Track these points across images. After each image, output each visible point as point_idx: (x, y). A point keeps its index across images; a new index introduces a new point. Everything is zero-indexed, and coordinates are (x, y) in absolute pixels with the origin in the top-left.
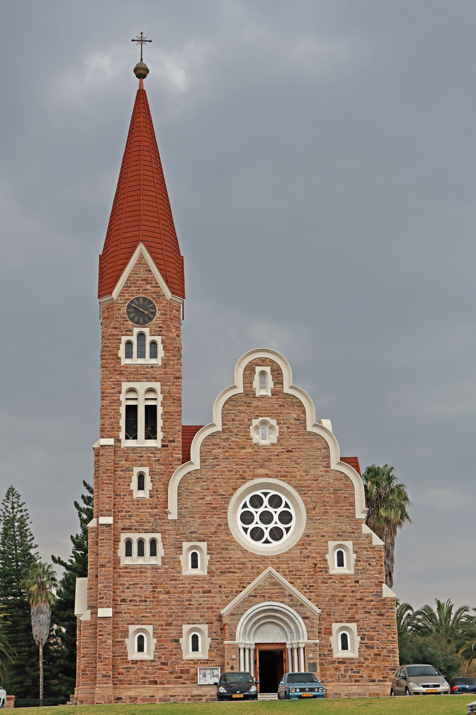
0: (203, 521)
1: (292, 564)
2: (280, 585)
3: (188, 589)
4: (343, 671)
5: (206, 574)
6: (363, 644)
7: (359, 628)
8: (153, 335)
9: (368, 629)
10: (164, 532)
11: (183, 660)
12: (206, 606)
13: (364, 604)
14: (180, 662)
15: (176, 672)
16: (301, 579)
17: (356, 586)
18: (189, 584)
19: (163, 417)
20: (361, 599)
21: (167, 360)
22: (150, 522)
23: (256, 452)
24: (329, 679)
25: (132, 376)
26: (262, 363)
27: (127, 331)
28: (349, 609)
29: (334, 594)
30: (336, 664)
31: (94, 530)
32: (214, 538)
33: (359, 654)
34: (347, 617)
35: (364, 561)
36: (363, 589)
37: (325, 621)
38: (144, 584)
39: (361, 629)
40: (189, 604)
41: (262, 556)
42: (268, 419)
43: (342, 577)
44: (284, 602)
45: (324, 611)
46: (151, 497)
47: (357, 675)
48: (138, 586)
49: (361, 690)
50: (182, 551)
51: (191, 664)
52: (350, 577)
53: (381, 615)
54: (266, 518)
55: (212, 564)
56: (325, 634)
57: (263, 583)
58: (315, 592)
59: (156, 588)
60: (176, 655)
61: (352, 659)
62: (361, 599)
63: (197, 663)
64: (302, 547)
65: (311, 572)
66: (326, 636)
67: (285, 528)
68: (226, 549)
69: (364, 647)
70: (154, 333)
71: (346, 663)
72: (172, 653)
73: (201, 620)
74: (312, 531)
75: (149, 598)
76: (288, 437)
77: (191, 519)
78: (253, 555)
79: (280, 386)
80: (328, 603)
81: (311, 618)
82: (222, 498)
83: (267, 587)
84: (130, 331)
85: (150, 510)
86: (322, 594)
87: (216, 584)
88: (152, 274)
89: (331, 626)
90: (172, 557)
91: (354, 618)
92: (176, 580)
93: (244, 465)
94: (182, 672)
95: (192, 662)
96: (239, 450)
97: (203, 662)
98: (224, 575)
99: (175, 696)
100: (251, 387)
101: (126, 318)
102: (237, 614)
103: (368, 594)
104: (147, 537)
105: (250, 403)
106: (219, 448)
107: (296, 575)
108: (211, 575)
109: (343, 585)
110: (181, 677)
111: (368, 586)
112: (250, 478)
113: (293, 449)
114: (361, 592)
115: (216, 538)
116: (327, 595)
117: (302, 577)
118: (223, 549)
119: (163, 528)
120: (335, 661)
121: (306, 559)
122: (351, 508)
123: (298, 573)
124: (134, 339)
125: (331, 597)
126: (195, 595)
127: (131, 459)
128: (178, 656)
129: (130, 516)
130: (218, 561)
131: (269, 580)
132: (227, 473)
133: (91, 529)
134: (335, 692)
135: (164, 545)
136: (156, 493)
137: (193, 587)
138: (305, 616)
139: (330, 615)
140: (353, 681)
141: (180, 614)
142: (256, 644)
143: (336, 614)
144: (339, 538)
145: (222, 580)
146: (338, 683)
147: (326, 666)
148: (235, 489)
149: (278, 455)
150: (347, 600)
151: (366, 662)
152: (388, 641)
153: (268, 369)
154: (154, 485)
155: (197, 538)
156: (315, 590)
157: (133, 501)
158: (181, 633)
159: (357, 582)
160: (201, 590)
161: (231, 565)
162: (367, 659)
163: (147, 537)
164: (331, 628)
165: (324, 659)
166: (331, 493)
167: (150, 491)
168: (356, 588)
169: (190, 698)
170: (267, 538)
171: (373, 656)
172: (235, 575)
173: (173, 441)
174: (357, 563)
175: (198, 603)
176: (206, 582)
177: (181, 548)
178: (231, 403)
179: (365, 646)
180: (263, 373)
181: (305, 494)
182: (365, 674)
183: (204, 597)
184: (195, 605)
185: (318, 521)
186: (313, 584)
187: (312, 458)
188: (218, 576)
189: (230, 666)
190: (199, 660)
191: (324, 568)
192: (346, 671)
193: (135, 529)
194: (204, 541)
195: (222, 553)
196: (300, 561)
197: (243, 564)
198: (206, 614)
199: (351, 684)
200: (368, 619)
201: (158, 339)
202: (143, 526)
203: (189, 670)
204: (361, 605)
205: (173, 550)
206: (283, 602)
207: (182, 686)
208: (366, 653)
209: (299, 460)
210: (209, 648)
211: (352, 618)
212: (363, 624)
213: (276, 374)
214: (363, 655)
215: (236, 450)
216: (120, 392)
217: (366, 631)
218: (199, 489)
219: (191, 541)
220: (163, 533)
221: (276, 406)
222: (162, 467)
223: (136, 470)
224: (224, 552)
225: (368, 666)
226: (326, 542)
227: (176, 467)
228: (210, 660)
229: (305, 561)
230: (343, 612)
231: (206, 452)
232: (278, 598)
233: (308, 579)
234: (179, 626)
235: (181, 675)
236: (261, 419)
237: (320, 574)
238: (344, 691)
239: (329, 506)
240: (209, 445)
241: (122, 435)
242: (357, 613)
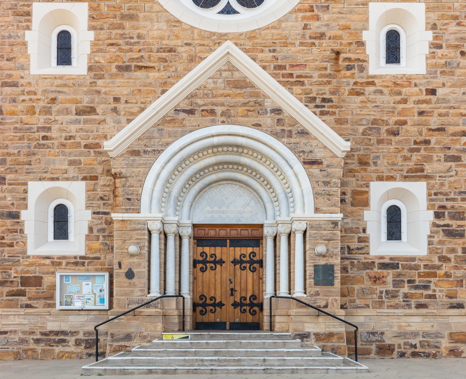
1: (282, 52)
2: (253, 87)
3: (41, 104)
4: (391, 285)
6: (438, 226)
7: (433, 192)
9: (452, 196)
11: (28, 257)
12: (83, 143)
13: (447, 141)
14: (21, 260)
15: (12, 282)
16: (302, 84)
18: (45, 91)
20: (441, 130)
24: (358, 302)
28: (412, 150)
29: (378, 117)
30: (376, 270)
33: (429, 249)
34: (405, 169)
35: (449, 46)
36: (445, 108)
37: (354, 176)
39: (436, 194)
40: (45, 138)
41: (214, 34)
43: (399, 82)
44: (260, 125)
45: (354, 156)
47: (422, 294)
51: (44, 265)
55: (100, 51)
56: (352, 205)
57: (211, 81)
58: (334, 113)
60: (11, 245)
62: (441, 130)
63: (60, 264)
64: (308, 14)
65: (326, 69)
66: (354, 209)
68: (131, 17)
69: (442, 232)
71: (398, 268)
72: (3, 241)
73: (72, 171)
78: (193, 33)
80: (364, 139)
83: (221, 92)
86: (349, 117)
87: (105, 93)
89: (368, 186)
90: (7, 34)
91: (422, 170)
94: (25, 281)
95: (48, 262)
97: (73, 260)
98: (126, 74)
99: (6, 333)
103: (456, 119)
107: (291, 75)
108: (95, 75)
109: (398, 98)
110: (22, 294)
111: (457, 101)
114: (440, 115)
116: (361, 119)
117: (306, 80)
118: (123, 17)
120: (373, 263)
121: (316, 42)
123: (296, 72)
125: (370, 126)
126: (59, 118)
128: (16, 247)
130: (112, 45)
131: (225, 74)
134: (370, 330)
137: (53, 100)
139: (367, 164)
140: (413, 306)
141: (22, 158)
142: (194, 226)
143: (379, 162)
146: (378, 310)
147: (352, 273)
150: (407, 131)
151: (444, 265)
156: (334, 110)
158: (25, 199)
159: (433, 92)
160: (73, 108)
161: (142, 54)
164: (367, 192)
165: (347, 259)
168: (431, 106)
169: (39, 337)
170: (228, 3)
171: (460, 253)
172: (153, 75)
174: (432, 50)
175: (64, 135)
176: (85, 89)
179: (443, 230)
182: (440, 291)
184: (56, 139)
186: (331, 96)
188: (112, 76)
190: (64, 258)
191: (358, 60)
192: (397, 283)
195: (121, 27)
196: (302, 44)
197: (170, 50)
198: (82, 159)
199: (408, 311)
200: (453, 173)
203: (42, 278)
204: (438, 143)
205: (11, 18)
207: (22, 311)
208: (445, 247)
210: (86, 232)
211: (417, 171)
212: (442, 185)
214: (439, 251)
217: (447, 200)
224: (127, 24)
225: (447, 275)
226: (363, 4)
228: (88, 258)
229: (314, 44)
230: (396, 157)
233: (320, 84)
234: (19, 184)
235: (23, 288)
237: (348, 73)
238: (391, 327)
242: (428, 159)
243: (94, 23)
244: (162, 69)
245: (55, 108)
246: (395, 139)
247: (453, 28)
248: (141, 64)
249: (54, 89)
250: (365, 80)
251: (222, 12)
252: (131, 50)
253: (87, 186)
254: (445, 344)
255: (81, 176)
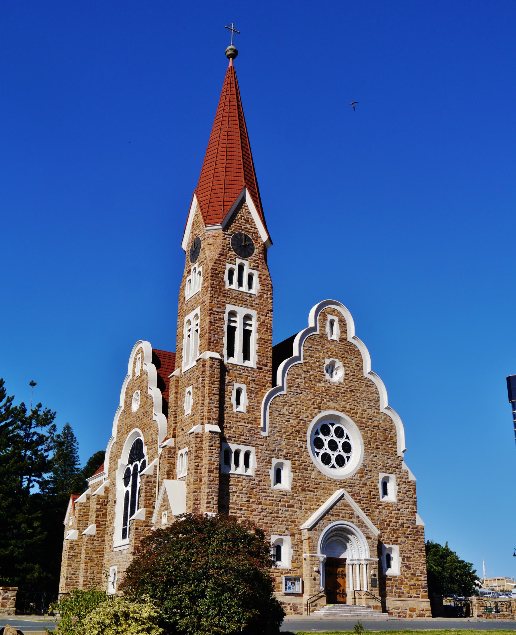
0: (289, 442)
5: (290, 490)
6: (403, 564)
8: (251, 269)
10: (257, 447)
17: (398, 514)
19: (258, 342)
21: (263, 293)
22: (246, 436)
23: (329, 387)
25: (235, 301)
26: (332, 313)
27: (231, 259)
28: (394, 533)
31: (200, 436)
32: (296, 458)
36: (403, 517)
38: (240, 493)
40: (277, 517)
42: (336, 360)
43: (389, 505)
46: (247, 412)
48: (236, 494)
49: (402, 604)
50: (271, 466)
52: (395, 505)
53: (415, 540)
54: (333, 445)
59: (250, 497)
61: (396, 577)
63: (282, 573)
64: (361, 475)
65: (367, 497)
67: (347, 457)
70: (253, 267)
74: (368, 462)
75: (245, 506)
76: (351, 379)
77: (279, 438)
79: (345, 335)
81: (373, 539)
82: (303, 423)
83: (341, 508)
84: (233, 260)
85: (246, 425)
88: (251, 216)
91: (397, 541)
92: (266, 492)
93: (319, 397)
96: (316, 383)
97: (287, 571)
98: (304, 492)
100: (325, 331)
101: (230, 248)
102: (319, 529)
104: (244, 449)
105: (324, 344)
106: (301, 378)
109: (389, 511)
112: (324, 408)
113: (354, 389)
114: (402, 519)
115: (298, 458)
118: (303, 469)
119: (256, 443)
122: (394, 446)
124: (236, 268)
126: (281, 508)
127: (232, 375)
129: (230, 427)
132: (307, 402)
133: (197, 434)
135: (257, 458)
136: (252, 409)
137: (280, 501)
138: (368, 536)
144: (386, 471)
145: (302, 496)
148: (313, 417)
149: (344, 393)
152: (420, 563)
153: (336, 319)
154: (250, 402)
155: (285, 456)
157: (233, 414)
161: (309, 484)
162: (407, 578)
163: (244, 449)
166: (381, 432)
167: (247, 407)
168: (399, 515)
171: (410, 575)
172: (312, 493)
173: (266, 365)
175: (283, 516)
176: (291, 497)
177: (271, 463)
178: (310, 341)
180: (332, 322)
181: (363, 429)
182: (405, 591)
183: (287, 510)
185: (372, 455)
187: (368, 400)
189: (313, 577)
190: (283, 570)
191: (377, 495)
193: (235, 441)
194: (289, 460)
197: (318, 484)
198: (290, 527)
201: (256, 273)
202: (240, 438)
204: (402, 530)
206: (352, 522)
209: (359, 400)
210: (291, 559)
213: (342, 324)
215: (313, 383)
216: (224, 313)
218: (286, 412)
219: (278, 458)
220: (257, 446)
221: (343, 350)
222: (257, 387)
223: (236, 386)
227: (268, 389)
231: (291, 380)
232: (349, 518)
236: (331, 359)
237: (374, 500)
238: (391, 605)
239: (380, 443)
240: (294, 374)
241: (225, 352)
243: (293, 470)
244: (316, 491)
245: (280, 504)
246: (389, 528)
247: (404, 486)
248: (309, 489)
249: (280, 496)
250: (379, 503)
251: (331, 467)
252: (305, 483)
253: (292, 539)
254: (408, 612)
255: (290, 534)
